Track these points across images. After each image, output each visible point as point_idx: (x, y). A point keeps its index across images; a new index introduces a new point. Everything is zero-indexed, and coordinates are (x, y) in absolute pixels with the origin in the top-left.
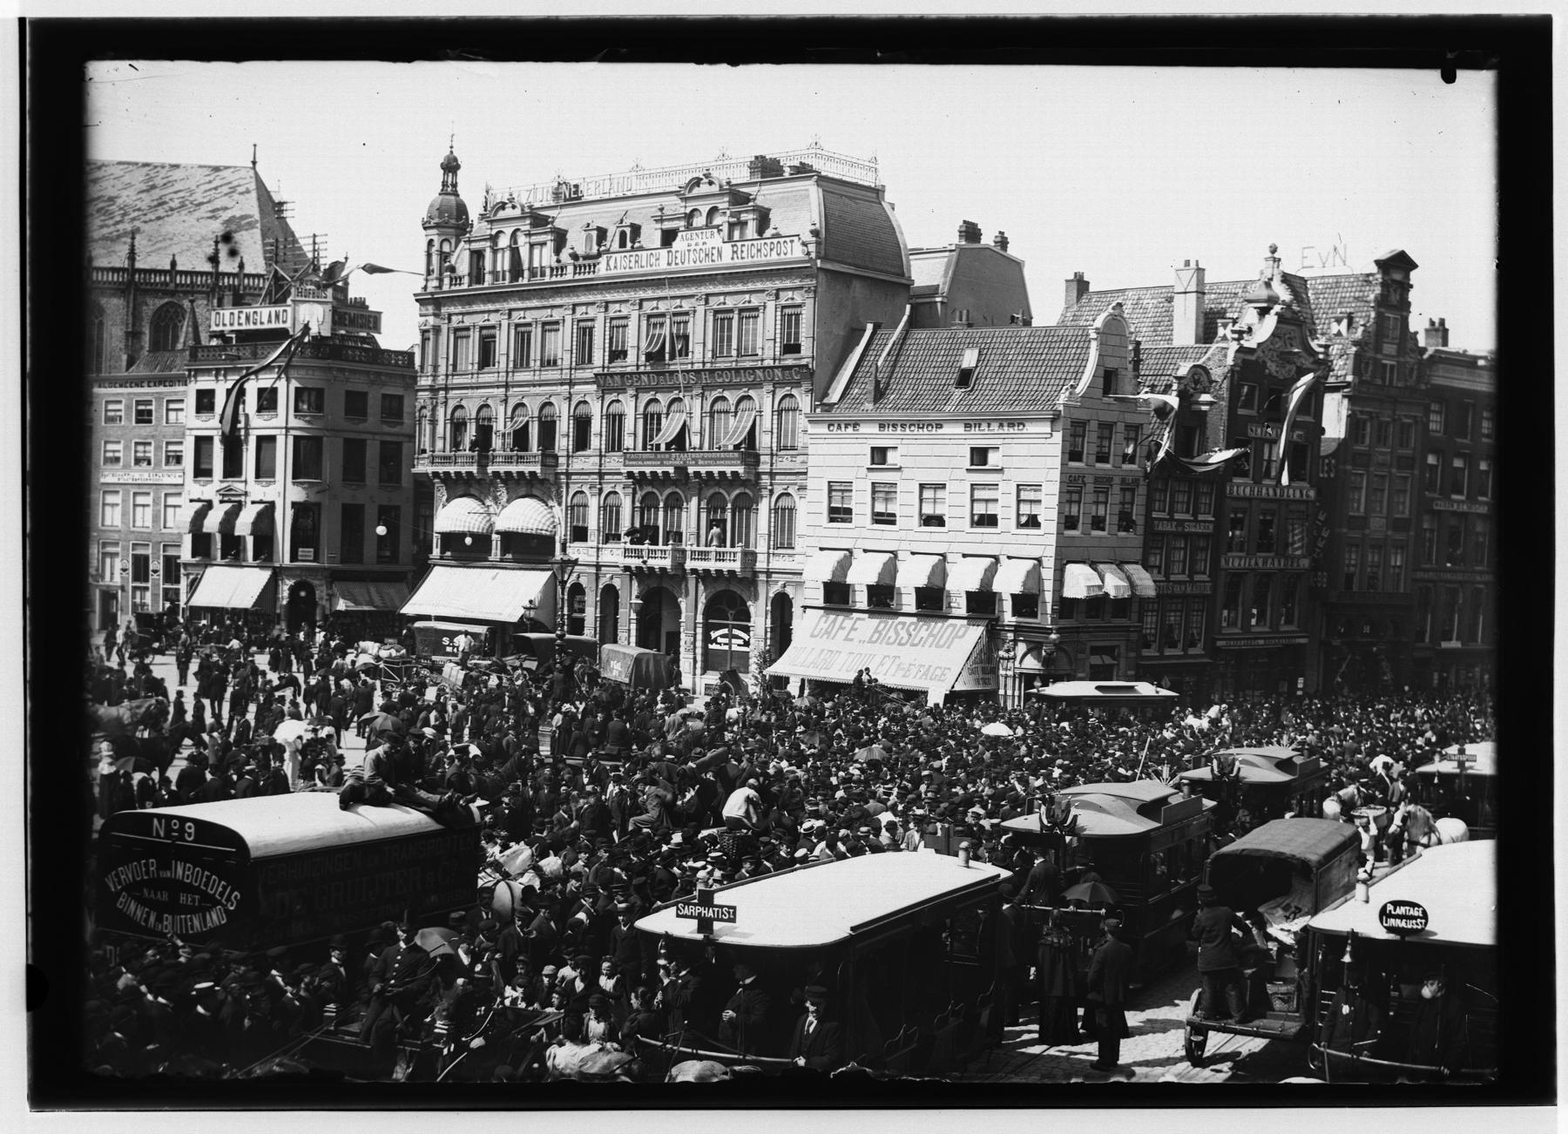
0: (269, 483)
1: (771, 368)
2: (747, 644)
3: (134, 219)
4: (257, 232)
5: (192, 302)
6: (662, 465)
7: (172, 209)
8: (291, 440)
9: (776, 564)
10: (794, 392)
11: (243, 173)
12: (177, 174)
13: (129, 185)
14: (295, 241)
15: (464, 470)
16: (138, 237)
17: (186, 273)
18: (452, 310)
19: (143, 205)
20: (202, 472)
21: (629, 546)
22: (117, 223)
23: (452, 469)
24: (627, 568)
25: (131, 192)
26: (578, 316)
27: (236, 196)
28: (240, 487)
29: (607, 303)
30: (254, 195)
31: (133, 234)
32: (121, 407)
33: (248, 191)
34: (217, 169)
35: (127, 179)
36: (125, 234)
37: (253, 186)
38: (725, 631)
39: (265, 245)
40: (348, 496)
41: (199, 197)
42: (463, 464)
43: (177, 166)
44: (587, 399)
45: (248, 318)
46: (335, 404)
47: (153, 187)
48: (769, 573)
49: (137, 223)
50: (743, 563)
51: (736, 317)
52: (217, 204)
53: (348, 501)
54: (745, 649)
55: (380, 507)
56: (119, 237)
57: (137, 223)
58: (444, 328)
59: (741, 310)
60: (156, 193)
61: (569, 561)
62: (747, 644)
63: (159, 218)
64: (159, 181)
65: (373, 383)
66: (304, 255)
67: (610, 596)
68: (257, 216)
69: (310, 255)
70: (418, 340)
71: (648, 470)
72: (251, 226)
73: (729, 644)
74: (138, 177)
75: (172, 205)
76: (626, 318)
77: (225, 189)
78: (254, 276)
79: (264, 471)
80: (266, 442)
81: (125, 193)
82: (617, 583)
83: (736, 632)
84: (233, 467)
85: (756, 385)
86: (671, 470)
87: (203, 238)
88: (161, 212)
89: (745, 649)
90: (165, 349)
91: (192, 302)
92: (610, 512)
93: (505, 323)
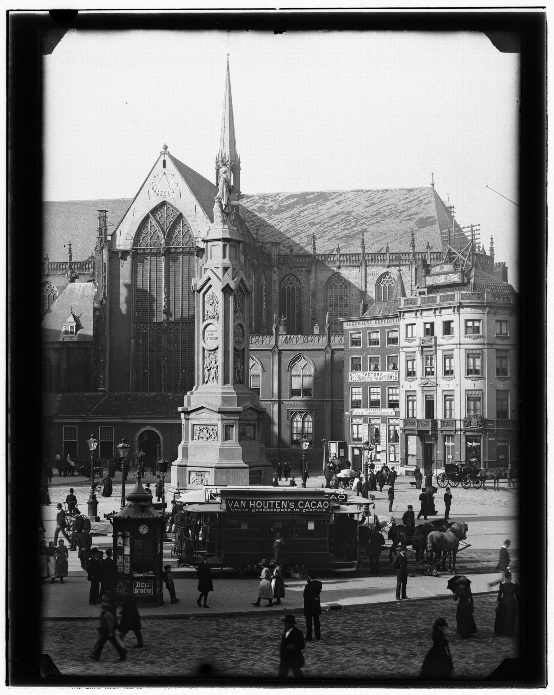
0: (451, 379)
3: (362, 224)
4: (437, 227)
5: (400, 271)
7: (385, 216)
11: (426, 192)
12: (387, 195)
13: (359, 204)
14: (460, 230)
16: (365, 234)
19: (368, 215)
22: (353, 227)
25: (359, 208)
27: (422, 206)
30: (433, 203)
31: (363, 232)
32: (361, 335)
33: (430, 202)
34: (410, 190)
35: (358, 200)
36: (358, 233)
37: (433, 199)
39: (442, 233)
41: (400, 208)
43: (387, 190)
47: (374, 204)
49: (365, 226)
52: (412, 211)
56: (354, 235)
57: (365, 226)
60: (375, 208)
63: (377, 222)
64: (376, 200)
66: (466, 237)
68: (436, 217)
69: (470, 238)
72: (433, 223)
74: (363, 199)
75: (384, 213)
77: (416, 202)
81: (356, 209)
87: (405, 232)
88: (378, 218)
90: (385, 300)
91: (400, 271)
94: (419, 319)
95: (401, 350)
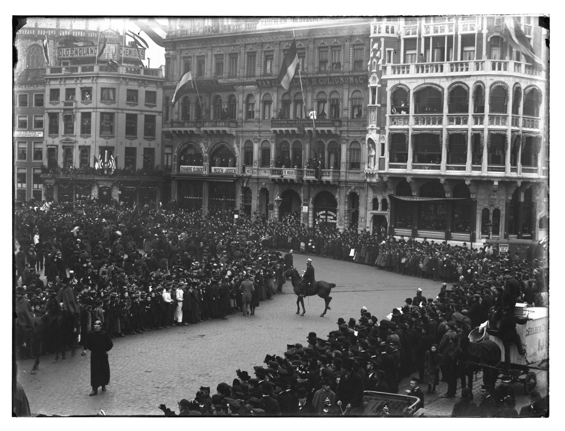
0: (88, 137)
1: (348, 76)
2: (335, 219)
6: (291, 127)
8: (99, 115)
9: (351, 178)
10: (360, 89)
15: (188, 129)
17: (43, 29)
18: (182, 47)
20: (54, 130)
21: (274, 168)
23: (182, 129)
24: (273, 180)
26: (248, 50)
28: (74, 139)
29: (246, 44)
38: (324, 212)
40: (128, 143)
42: (188, 127)
44: (253, 93)
45: (76, 52)
46: (122, 95)
48: (346, 182)
50: (333, 176)
51: (329, 50)
53: (128, 146)
54: (334, 221)
55: (145, 149)
58: (178, 57)
59: (332, 47)
61: (246, 177)
62: (335, 219)
65: (140, 86)
67: (264, 193)
70: (164, 63)
71: (283, 129)
73: (326, 219)
76: (272, 51)
78: (78, 31)
79: (86, 130)
80: (86, 116)
82: (268, 187)
83: (330, 212)
84: (69, 129)
85: (341, 85)
86: (296, 129)
89: (334, 221)
92: (265, 152)
93: (210, 53)
94: (63, 86)
95: (46, 111)
